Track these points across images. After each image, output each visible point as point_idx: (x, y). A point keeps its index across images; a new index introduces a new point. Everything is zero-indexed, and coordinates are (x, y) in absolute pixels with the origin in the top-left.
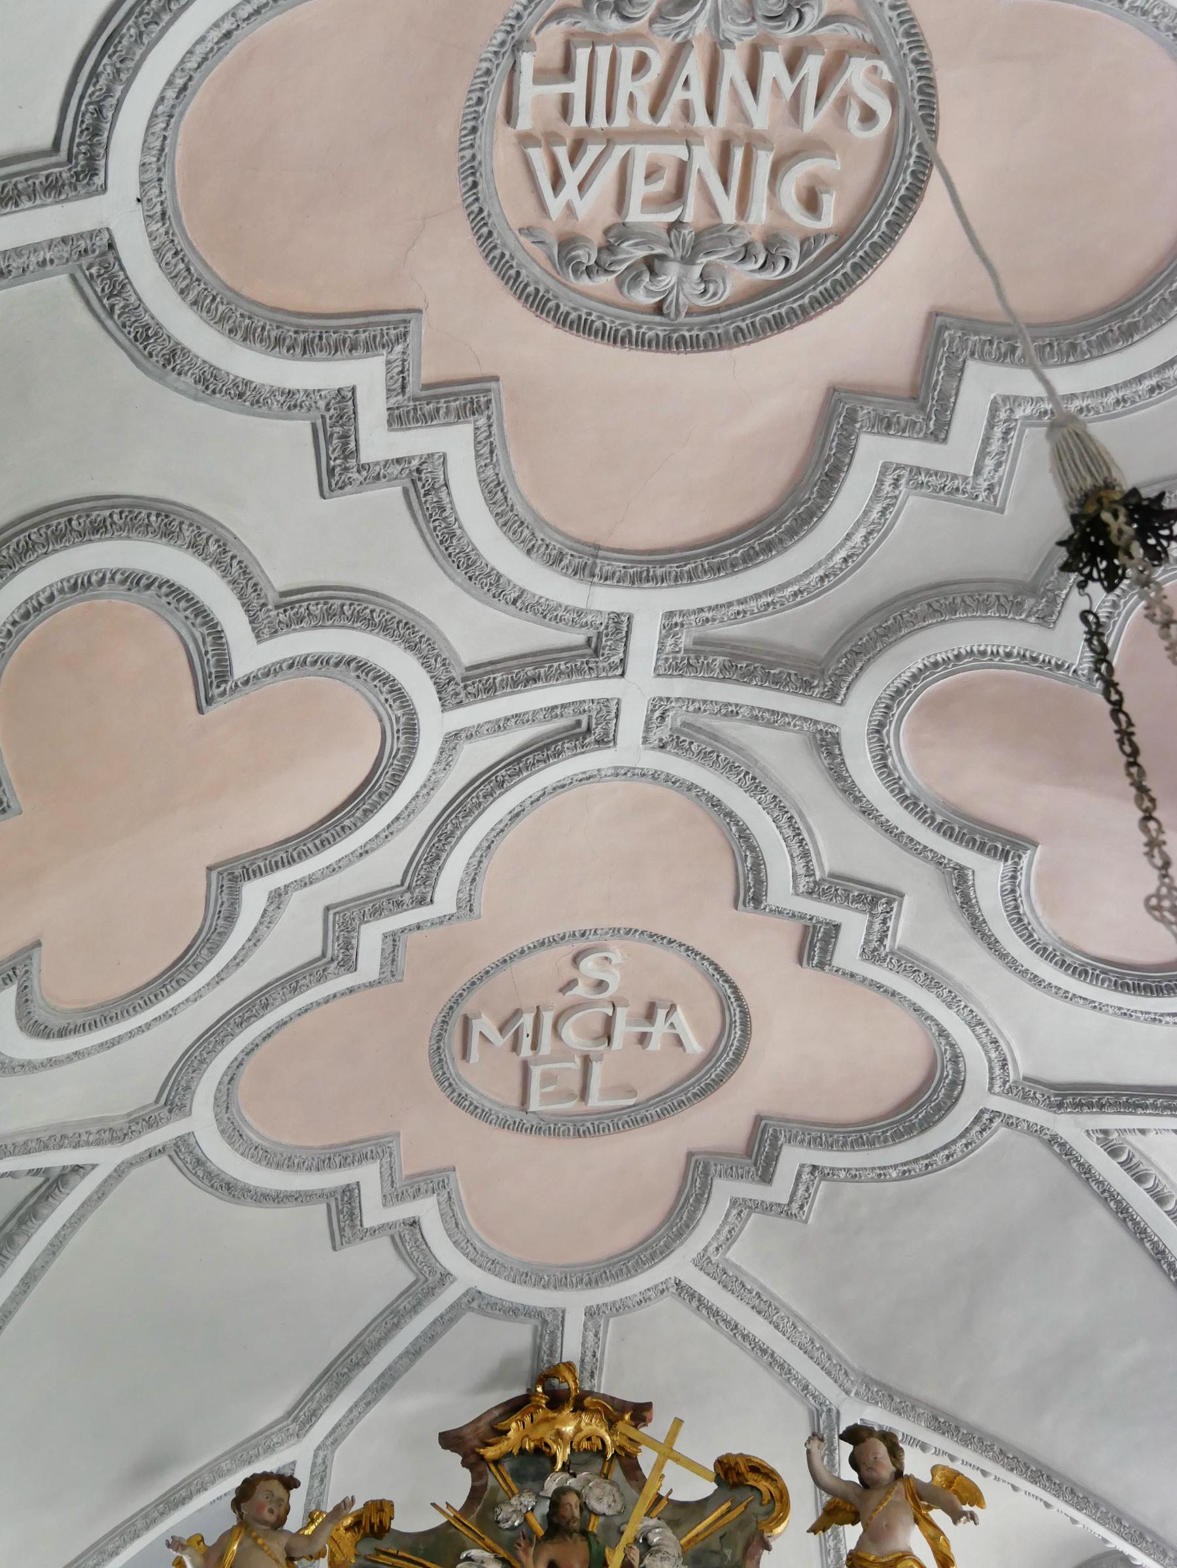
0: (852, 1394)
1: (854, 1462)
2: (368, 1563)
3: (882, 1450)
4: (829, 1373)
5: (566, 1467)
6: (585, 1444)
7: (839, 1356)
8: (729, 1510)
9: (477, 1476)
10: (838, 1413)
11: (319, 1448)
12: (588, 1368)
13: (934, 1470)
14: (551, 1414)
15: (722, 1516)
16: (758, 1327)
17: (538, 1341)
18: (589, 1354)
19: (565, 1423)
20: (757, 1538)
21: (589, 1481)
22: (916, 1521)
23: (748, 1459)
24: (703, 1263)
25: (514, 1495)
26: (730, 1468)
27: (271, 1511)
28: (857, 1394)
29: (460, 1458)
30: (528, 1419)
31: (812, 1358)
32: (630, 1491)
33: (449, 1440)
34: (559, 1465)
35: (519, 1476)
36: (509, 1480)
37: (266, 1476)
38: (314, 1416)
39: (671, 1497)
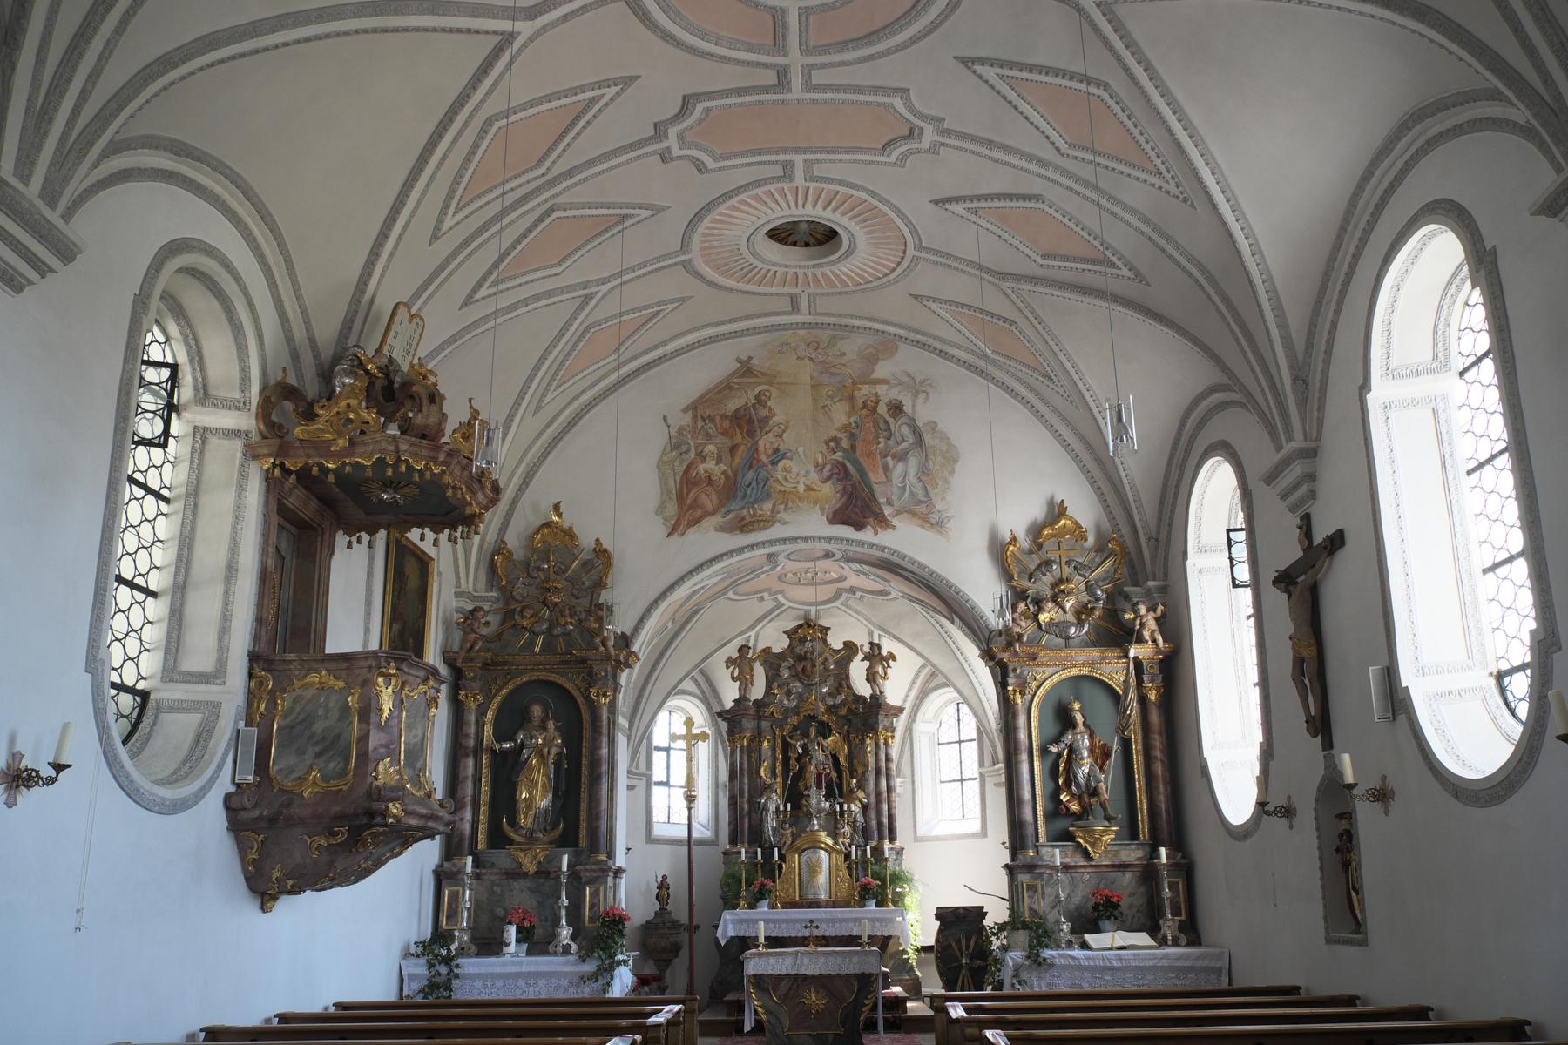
16: (856, 615)
24: (842, 604)
35: (800, 641)
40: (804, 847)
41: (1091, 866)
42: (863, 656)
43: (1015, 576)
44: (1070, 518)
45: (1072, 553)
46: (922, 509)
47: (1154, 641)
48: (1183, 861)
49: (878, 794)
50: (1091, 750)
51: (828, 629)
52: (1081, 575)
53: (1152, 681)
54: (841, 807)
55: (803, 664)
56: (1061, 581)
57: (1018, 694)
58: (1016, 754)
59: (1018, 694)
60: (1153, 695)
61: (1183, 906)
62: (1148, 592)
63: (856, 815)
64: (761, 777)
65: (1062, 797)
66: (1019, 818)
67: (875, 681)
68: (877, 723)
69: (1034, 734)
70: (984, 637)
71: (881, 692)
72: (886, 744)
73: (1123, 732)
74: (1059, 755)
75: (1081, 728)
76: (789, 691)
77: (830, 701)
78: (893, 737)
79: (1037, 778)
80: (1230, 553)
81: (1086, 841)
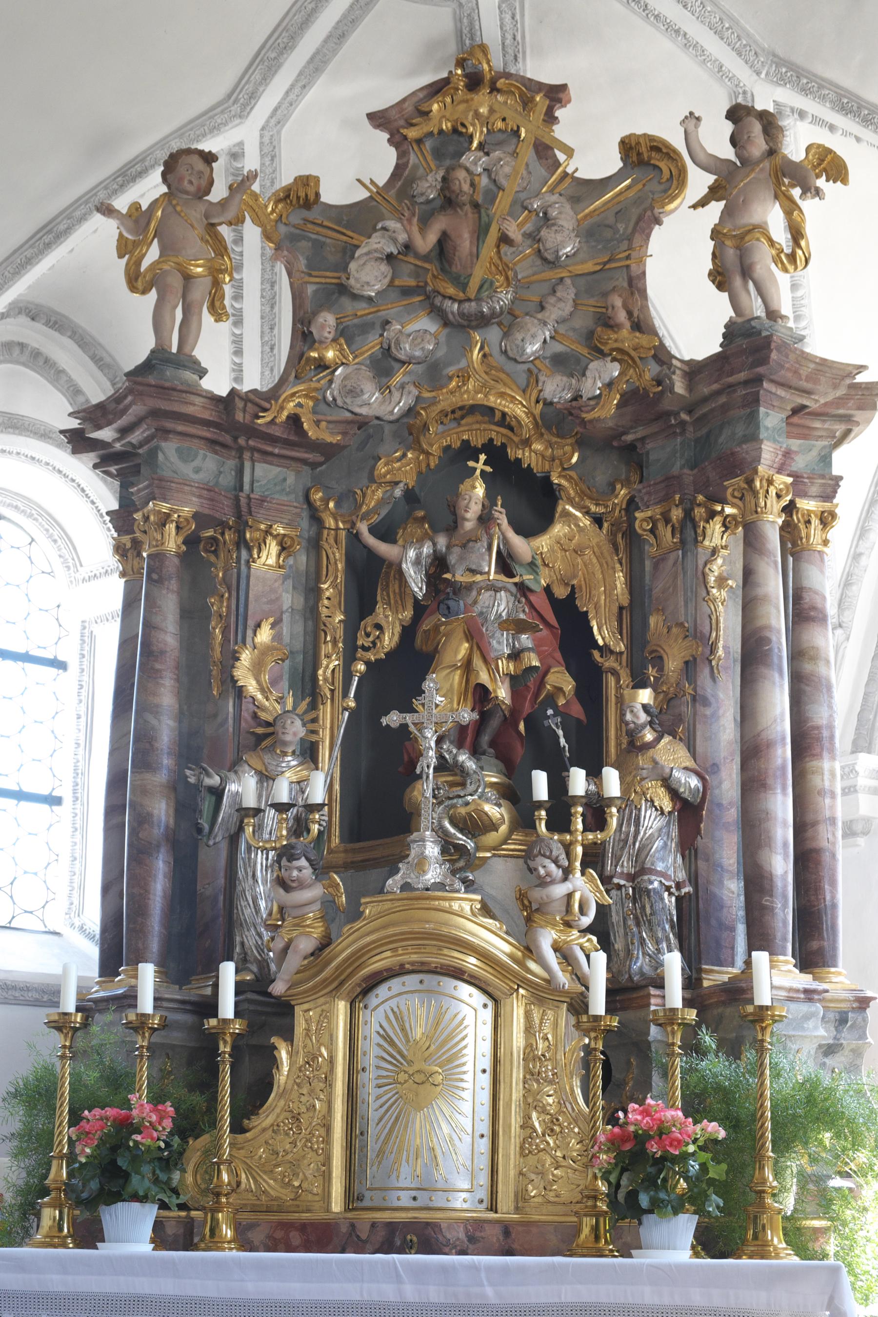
0: (763, 75)
1: (734, 141)
2: (298, 231)
3: (757, 128)
4: (740, 54)
6: (500, 125)
7: (748, 35)
9: (402, 155)
10: (752, 95)
11: (263, 129)
12: (510, 51)
13: (808, 149)
14: (469, 96)
17: (459, 25)
18: (509, 37)
19: (481, 105)
20: (649, 213)
21: (501, 159)
22: (776, 197)
23: (651, 138)
25: (431, 171)
26: (631, 148)
27: (191, 182)
28: (767, 74)
29: (386, 136)
30: (448, 100)
31: (722, 39)
32: (540, 171)
33: (378, 119)
34: (475, 144)
35: (438, 154)
36: (429, 158)
37: (189, 152)
38: (254, 96)
39: (576, 175)
40: (377, 964)
54: (558, 785)
64: (240, 692)
67: (746, 272)
68: (753, 437)
71: (773, 315)
76: (387, 352)
78: (827, 519)
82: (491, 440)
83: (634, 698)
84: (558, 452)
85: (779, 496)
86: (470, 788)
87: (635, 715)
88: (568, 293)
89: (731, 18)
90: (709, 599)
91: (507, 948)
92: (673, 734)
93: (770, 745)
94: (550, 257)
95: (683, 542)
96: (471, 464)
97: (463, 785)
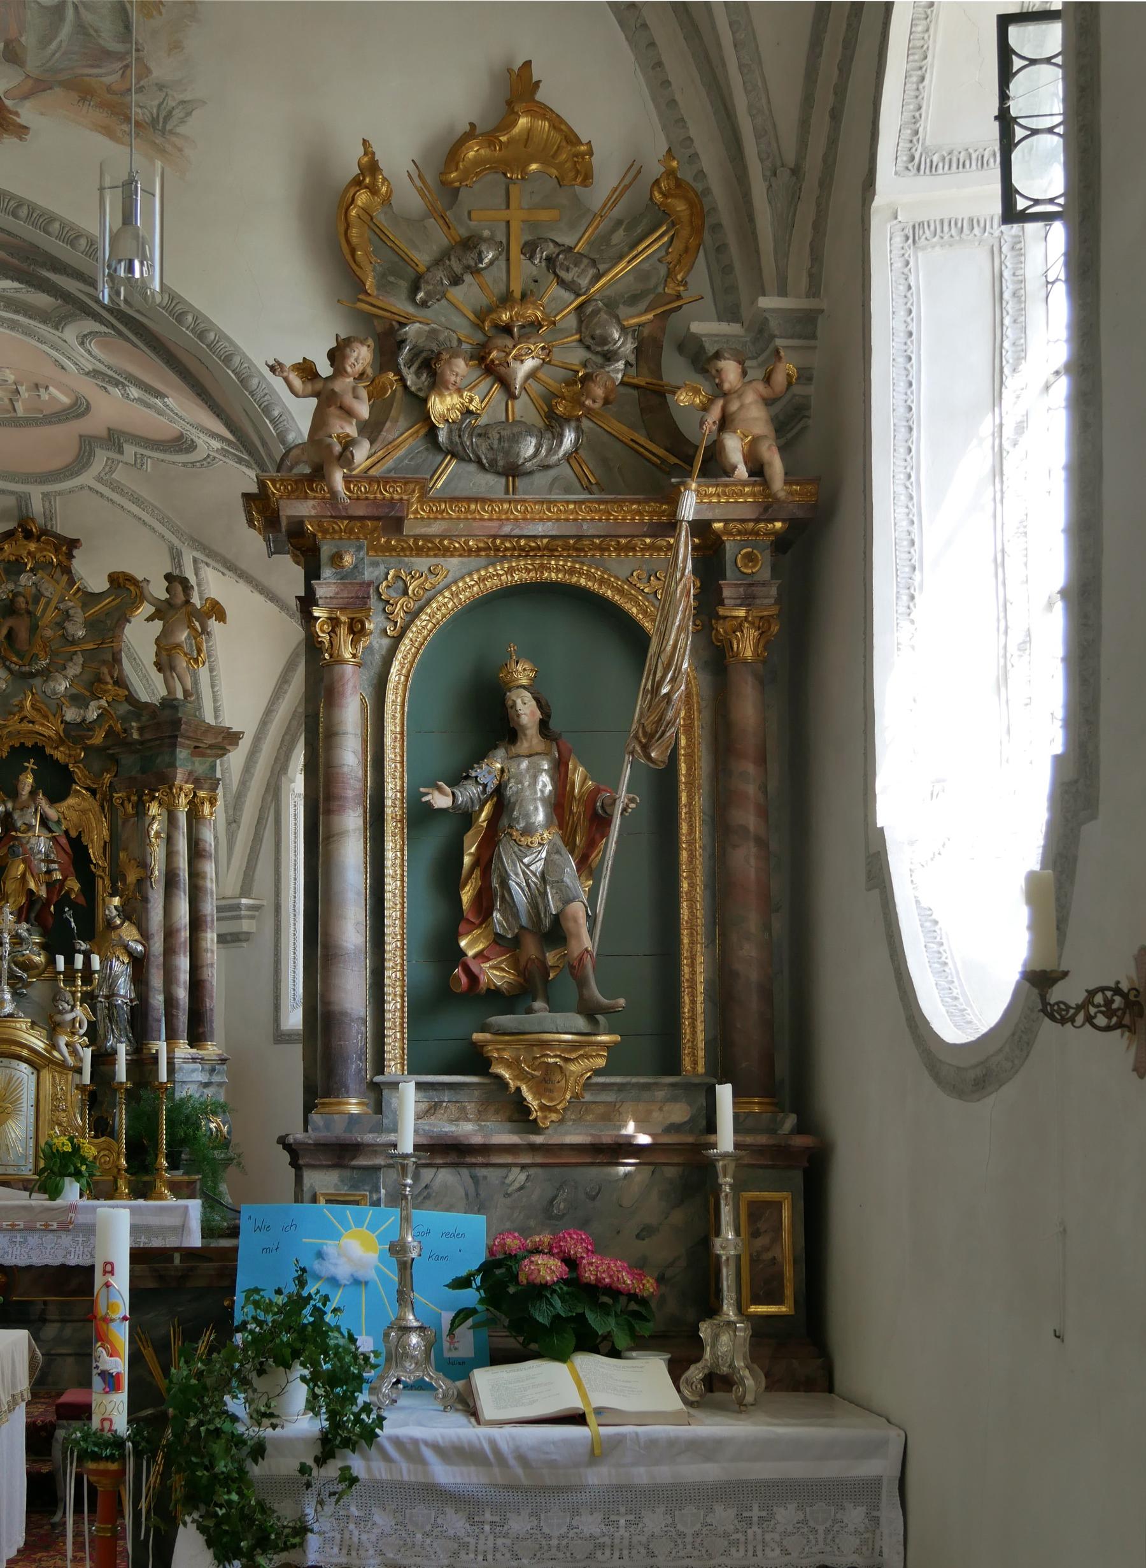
1: (168, 590)
3: (179, 588)
5: (32, 570)
8: (113, 600)
15: (109, 603)
16: (135, 509)
24: (99, 479)
41: (533, 1148)
42: (152, 609)
43: (369, 283)
44: (543, 111)
45: (544, 215)
46: (109, 76)
47: (758, 470)
48: (799, 1141)
49: (170, 933)
50: (559, 804)
51: (73, 544)
52: (562, 282)
53: (747, 600)
55: (10, 622)
56: (506, 300)
57: (343, 631)
58: (329, 812)
59: (343, 631)
60: (747, 646)
61: (788, 1271)
62: (761, 332)
63: (117, 977)
65: (463, 944)
66: (327, 1003)
67: (172, 668)
68: (172, 765)
69: (389, 754)
70: (273, 460)
72: (194, 816)
73: (645, 748)
74: (464, 818)
75: (532, 739)
77: (71, 714)
79: (392, 886)
80: (1004, 97)
81: (521, 1075)
82: (36, 743)
83: (111, 901)
84: (73, 753)
85: (186, 795)
86: (25, 947)
87: (110, 912)
88: (79, 659)
89: (168, 518)
90: (150, 844)
91: (42, 1045)
92: (130, 919)
93: (178, 931)
94: (70, 639)
95: (137, 812)
96: (26, 764)
97: (21, 944)
